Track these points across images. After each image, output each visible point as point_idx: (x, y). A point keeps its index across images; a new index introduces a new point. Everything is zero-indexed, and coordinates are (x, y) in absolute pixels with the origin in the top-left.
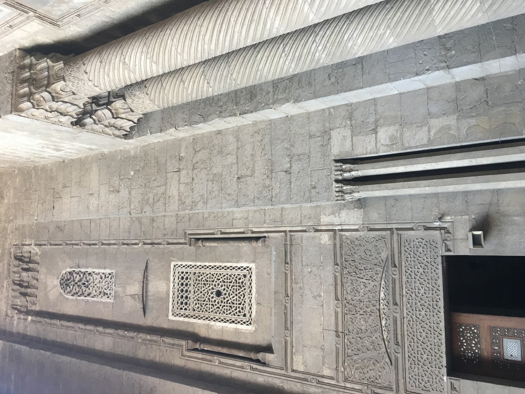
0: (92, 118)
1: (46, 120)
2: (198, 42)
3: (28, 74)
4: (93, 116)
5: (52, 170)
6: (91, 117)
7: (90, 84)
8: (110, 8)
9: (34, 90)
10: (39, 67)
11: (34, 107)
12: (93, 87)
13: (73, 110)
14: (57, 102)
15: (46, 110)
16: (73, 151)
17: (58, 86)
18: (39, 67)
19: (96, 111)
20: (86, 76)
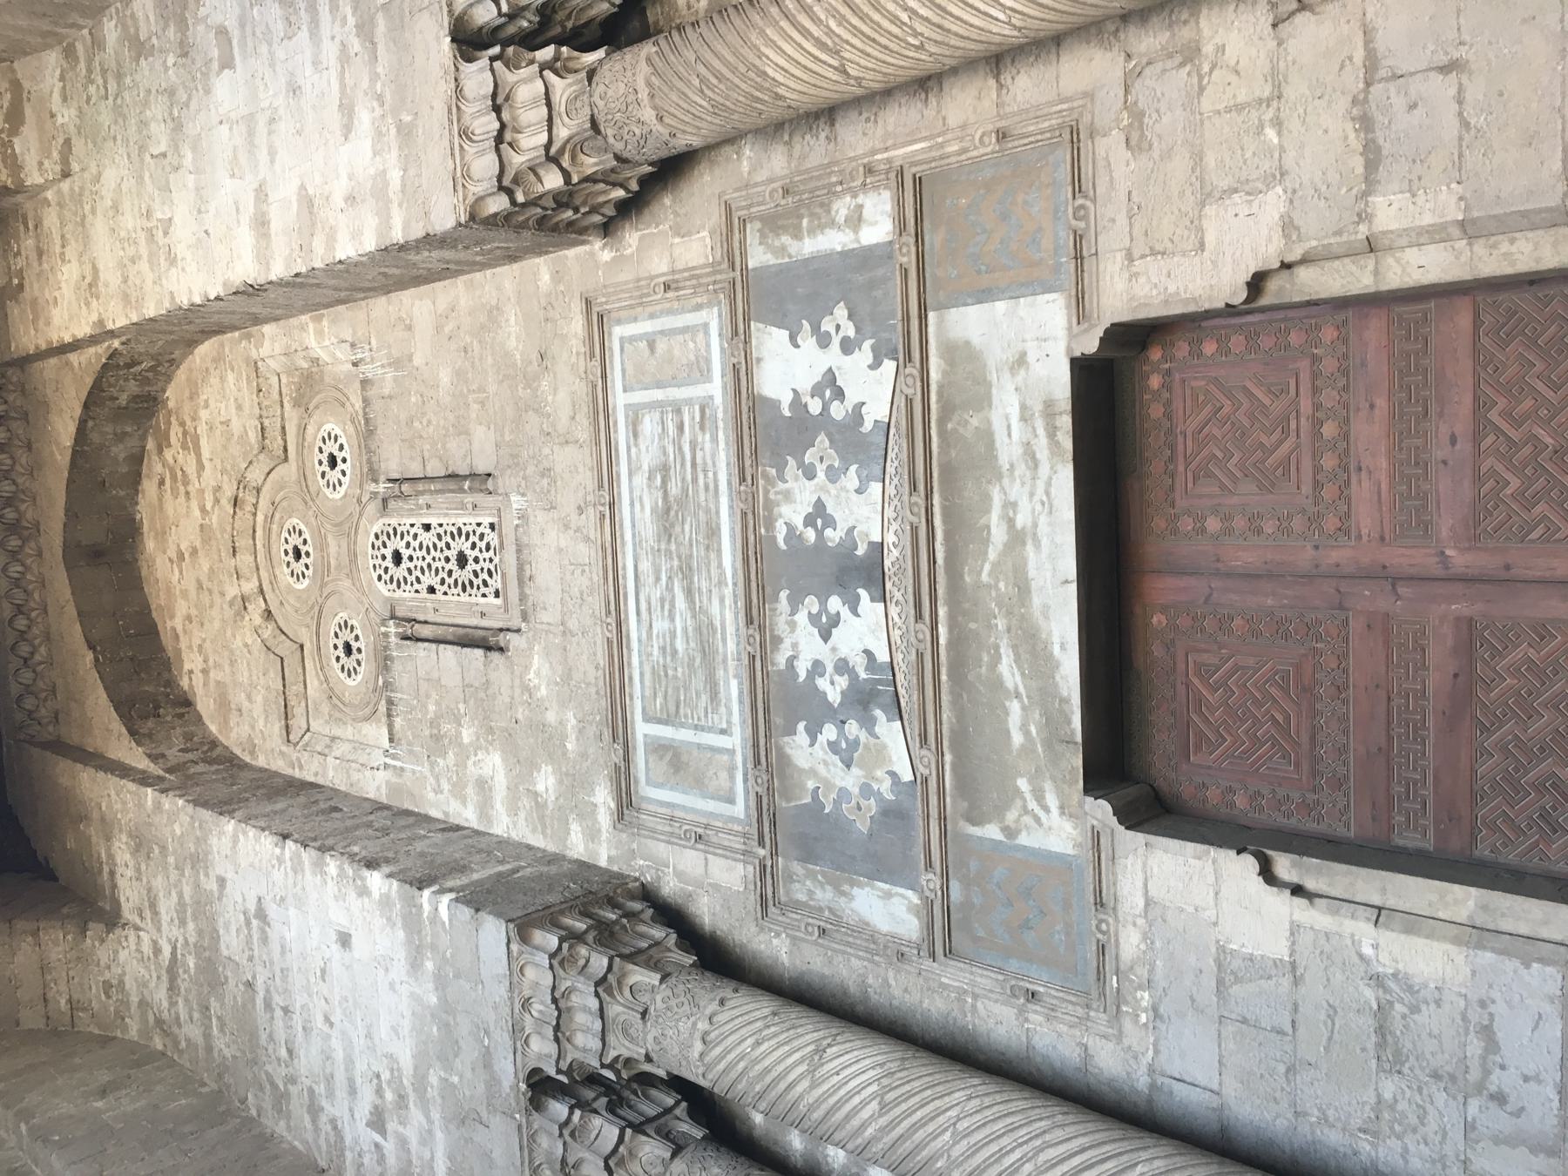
0: (571, 1113)
1: (517, 1007)
2: (1021, 1145)
3: (614, 917)
4: (577, 1113)
5: (276, 1157)
6: (571, 1109)
7: (703, 1026)
8: (891, 974)
9: (590, 938)
10: (642, 928)
11: (552, 956)
12: (698, 1035)
13: (585, 1045)
14: (597, 995)
15: (554, 988)
16: (391, 1160)
17: (640, 976)
18: (642, 928)
19: (596, 1112)
20: (714, 1006)
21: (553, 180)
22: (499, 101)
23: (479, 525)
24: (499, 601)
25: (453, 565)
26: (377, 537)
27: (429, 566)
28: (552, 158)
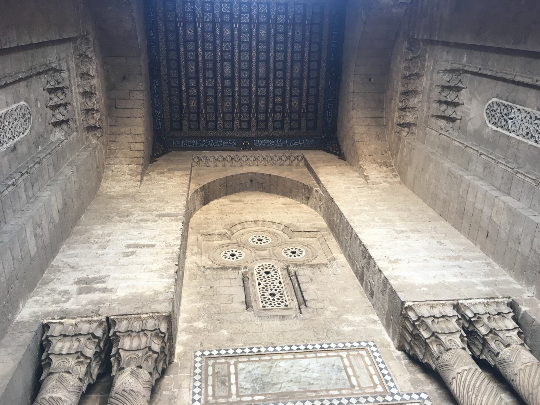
21: (425, 334)
22: (446, 318)
23: (286, 301)
24: (261, 308)
25: (270, 292)
26: (273, 266)
27: (267, 283)
28: (433, 334)
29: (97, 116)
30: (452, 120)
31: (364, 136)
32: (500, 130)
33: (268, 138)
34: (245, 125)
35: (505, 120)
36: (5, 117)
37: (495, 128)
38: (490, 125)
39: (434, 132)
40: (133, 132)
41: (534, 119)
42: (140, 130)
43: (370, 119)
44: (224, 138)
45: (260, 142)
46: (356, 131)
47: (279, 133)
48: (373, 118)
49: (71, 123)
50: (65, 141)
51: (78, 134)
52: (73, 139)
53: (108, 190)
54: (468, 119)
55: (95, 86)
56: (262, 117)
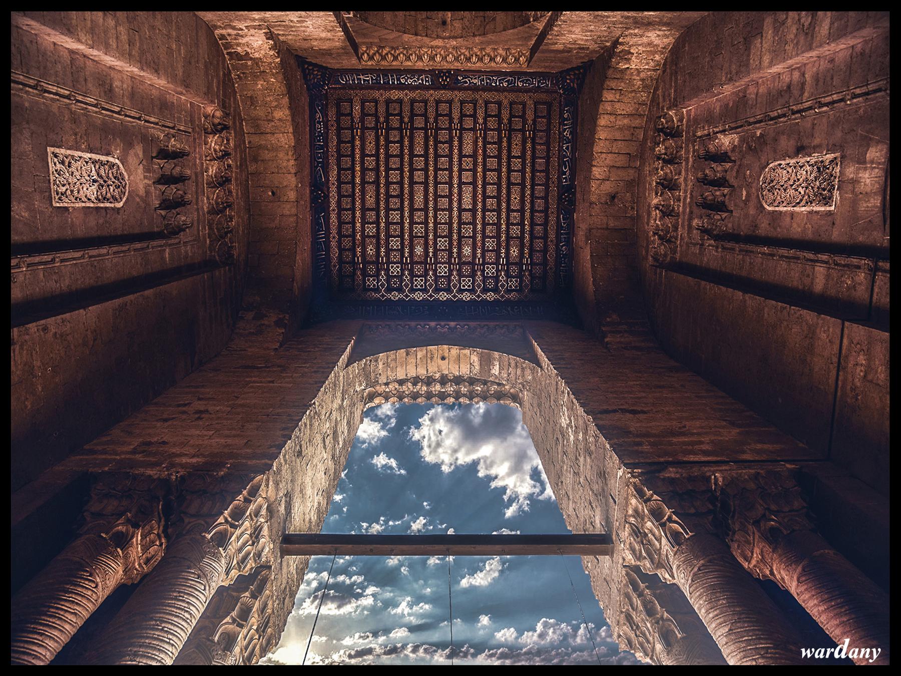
29: (660, 149)
30: (165, 154)
31: (274, 104)
32: (103, 158)
33: (411, 88)
34: (444, 108)
35: (101, 177)
36: (801, 200)
37: (111, 159)
38: (117, 161)
39: (182, 128)
40: (612, 118)
41: (69, 192)
42: (603, 121)
43: (268, 130)
44: (475, 89)
45: (422, 80)
46: (287, 112)
47: (395, 94)
48: (262, 133)
49: (702, 152)
50: (716, 130)
51: (695, 132)
52: (704, 127)
53: (667, 33)
54: (144, 162)
55: (657, 194)
56: (419, 122)
